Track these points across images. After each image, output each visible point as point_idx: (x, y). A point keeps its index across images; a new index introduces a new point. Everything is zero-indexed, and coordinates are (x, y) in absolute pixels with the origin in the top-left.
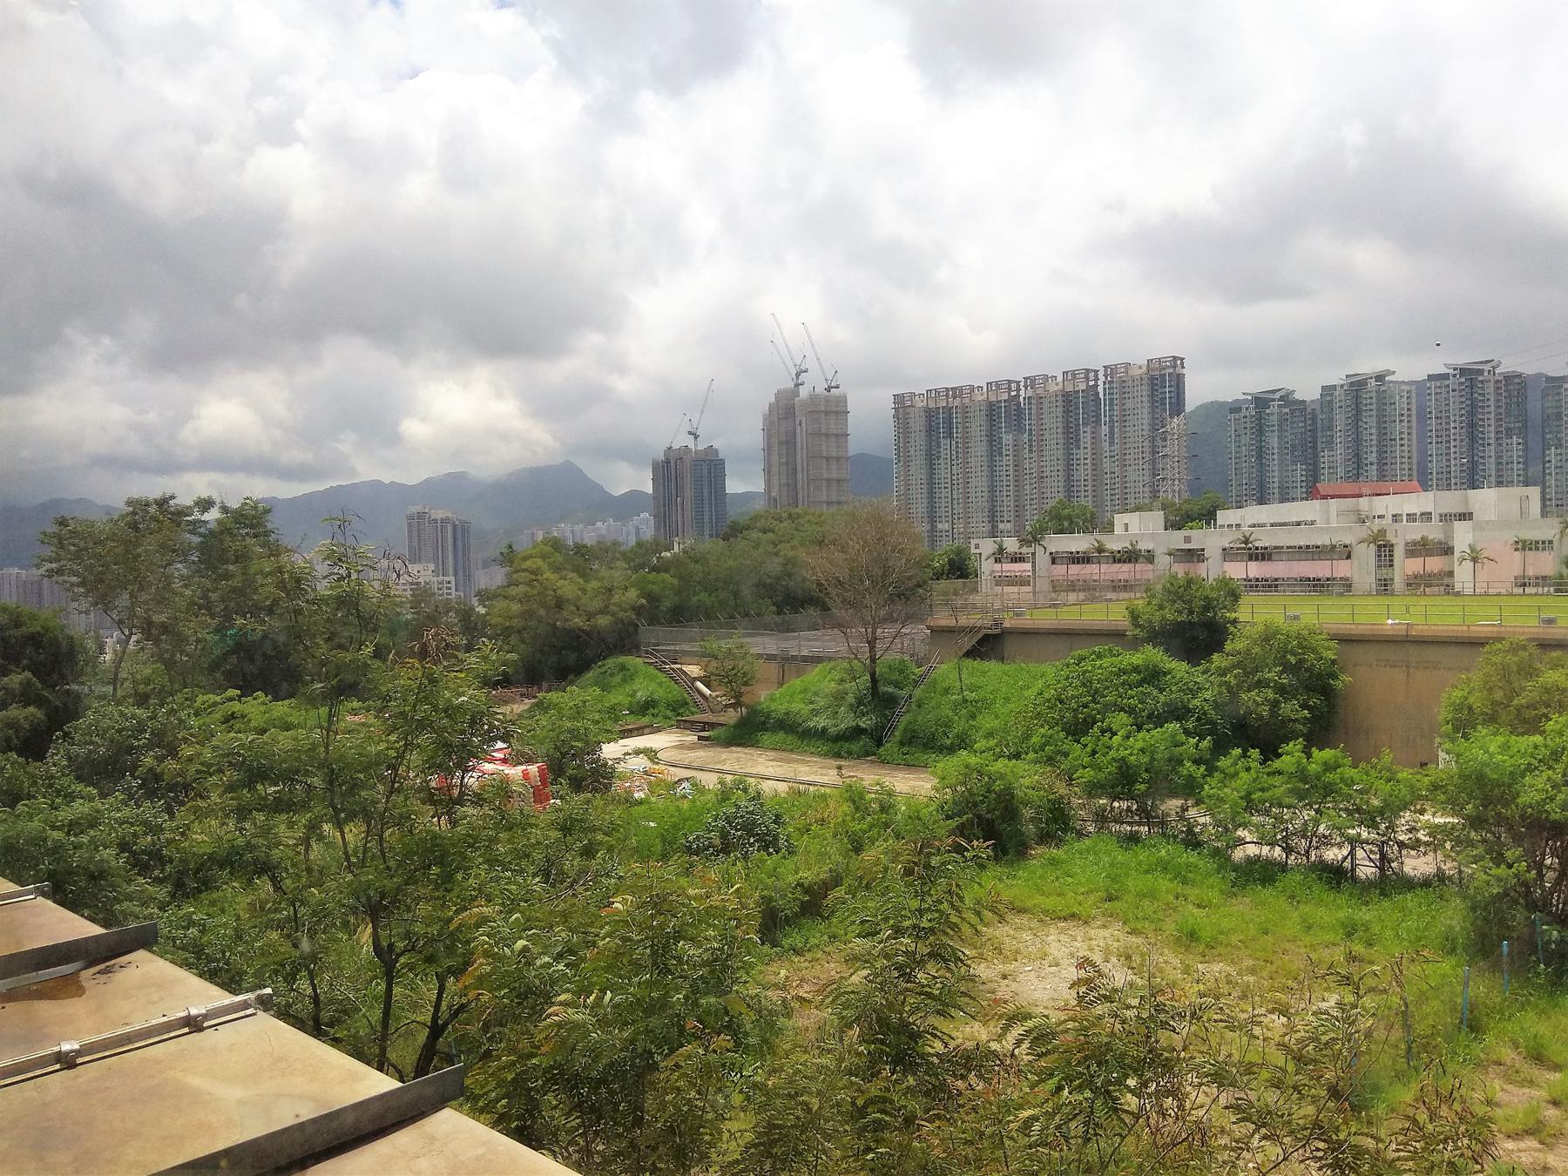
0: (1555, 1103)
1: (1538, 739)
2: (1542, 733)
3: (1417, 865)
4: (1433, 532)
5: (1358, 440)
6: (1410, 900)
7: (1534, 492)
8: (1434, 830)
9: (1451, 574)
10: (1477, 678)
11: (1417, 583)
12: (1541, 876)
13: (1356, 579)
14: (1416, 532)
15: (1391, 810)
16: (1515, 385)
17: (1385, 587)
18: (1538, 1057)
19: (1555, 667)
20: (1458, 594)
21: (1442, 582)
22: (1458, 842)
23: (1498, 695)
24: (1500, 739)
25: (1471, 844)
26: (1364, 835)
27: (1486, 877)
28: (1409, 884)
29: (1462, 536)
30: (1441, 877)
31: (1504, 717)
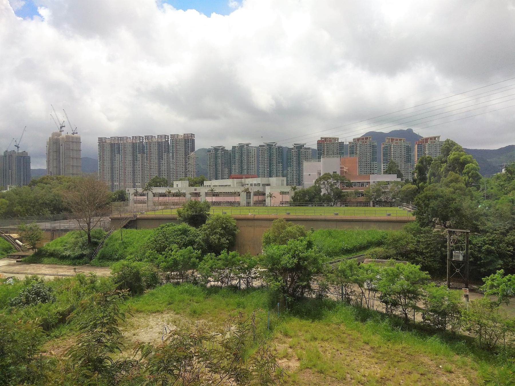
0: (291, 347)
1: (285, 246)
2: (287, 244)
3: (256, 283)
4: (260, 189)
5: (242, 162)
6: (254, 294)
7: (285, 179)
8: (261, 273)
9: (265, 201)
10: (271, 229)
11: (256, 203)
12: (287, 284)
13: (241, 202)
14: (256, 189)
15: (250, 268)
16: (280, 149)
17: (248, 204)
18: (286, 335)
19: (290, 226)
20: (266, 206)
21: (262, 203)
22: (267, 276)
23: (276, 234)
24: (277, 246)
25: (270, 276)
26: (243, 276)
27: (274, 285)
28: (254, 289)
29: (268, 190)
30: (262, 286)
31: (278, 240)
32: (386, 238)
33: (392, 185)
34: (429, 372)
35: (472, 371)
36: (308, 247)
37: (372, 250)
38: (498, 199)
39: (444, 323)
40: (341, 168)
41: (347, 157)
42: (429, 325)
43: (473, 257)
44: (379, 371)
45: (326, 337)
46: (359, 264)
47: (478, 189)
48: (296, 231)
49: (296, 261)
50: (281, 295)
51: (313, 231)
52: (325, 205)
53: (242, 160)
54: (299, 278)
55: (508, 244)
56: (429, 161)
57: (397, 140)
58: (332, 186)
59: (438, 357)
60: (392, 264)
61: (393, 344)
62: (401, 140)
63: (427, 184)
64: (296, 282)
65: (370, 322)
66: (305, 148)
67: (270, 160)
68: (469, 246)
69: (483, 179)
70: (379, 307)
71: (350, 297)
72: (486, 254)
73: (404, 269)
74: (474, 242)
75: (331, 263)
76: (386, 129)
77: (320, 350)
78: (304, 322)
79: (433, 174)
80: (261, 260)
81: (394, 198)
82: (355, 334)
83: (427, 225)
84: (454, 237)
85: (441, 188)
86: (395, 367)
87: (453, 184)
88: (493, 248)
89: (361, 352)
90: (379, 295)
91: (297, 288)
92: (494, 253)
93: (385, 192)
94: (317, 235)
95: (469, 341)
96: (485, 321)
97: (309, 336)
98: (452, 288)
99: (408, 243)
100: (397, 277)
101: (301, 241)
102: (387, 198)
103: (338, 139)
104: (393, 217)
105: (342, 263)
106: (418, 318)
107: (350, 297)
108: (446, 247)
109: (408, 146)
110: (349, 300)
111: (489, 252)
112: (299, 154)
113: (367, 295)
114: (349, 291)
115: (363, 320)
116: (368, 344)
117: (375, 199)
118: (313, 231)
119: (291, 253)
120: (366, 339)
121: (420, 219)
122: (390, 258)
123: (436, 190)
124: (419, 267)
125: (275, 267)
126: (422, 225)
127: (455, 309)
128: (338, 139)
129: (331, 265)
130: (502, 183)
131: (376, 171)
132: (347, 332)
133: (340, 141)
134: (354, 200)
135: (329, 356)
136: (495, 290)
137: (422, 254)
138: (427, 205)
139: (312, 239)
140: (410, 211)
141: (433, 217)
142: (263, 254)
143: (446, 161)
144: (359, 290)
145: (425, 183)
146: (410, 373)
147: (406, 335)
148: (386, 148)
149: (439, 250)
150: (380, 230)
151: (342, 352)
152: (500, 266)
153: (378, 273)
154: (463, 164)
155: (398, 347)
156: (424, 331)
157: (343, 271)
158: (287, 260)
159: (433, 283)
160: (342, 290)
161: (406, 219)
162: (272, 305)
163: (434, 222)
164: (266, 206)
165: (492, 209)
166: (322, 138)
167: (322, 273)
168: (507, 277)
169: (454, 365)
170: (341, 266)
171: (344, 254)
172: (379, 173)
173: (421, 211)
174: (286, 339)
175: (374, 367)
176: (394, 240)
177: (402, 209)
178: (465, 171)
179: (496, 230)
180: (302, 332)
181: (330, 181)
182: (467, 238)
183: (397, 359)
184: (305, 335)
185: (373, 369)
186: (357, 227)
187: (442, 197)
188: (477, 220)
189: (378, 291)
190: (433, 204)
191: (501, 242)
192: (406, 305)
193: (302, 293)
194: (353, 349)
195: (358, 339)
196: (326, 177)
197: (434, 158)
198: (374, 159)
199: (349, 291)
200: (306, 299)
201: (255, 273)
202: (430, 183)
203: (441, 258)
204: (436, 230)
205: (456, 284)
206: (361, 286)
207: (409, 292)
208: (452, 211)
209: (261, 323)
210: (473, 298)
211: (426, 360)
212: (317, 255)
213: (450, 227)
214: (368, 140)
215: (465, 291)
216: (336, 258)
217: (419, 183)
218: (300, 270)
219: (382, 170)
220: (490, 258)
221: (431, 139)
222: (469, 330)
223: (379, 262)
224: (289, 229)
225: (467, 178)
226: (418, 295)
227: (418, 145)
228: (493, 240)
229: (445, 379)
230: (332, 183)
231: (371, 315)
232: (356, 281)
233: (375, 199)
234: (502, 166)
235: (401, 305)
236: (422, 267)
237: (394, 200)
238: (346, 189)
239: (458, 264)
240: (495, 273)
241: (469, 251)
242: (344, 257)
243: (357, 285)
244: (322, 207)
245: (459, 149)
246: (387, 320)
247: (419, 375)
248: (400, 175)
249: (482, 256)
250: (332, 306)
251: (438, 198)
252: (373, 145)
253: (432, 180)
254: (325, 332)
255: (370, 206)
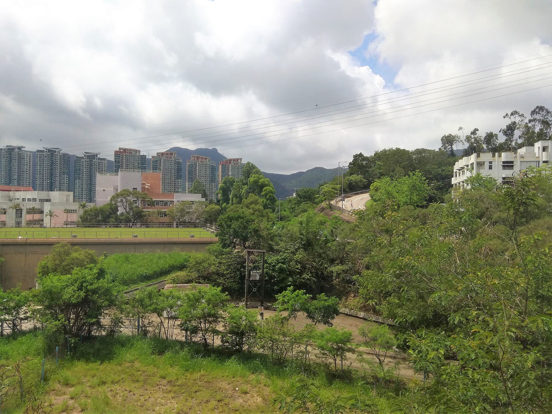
0: (72, 398)
1: (69, 276)
2: (71, 274)
3: (26, 326)
4: (37, 205)
5: (10, 170)
6: (23, 339)
7: (71, 194)
8: (34, 311)
9: (42, 220)
10: (50, 256)
11: (30, 223)
12: (69, 322)
13: (7, 222)
14: (31, 205)
15: (18, 306)
16: (66, 158)
17: (18, 224)
18: (67, 384)
19: (76, 251)
20: (45, 227)
21: (40, 223)
22: (42, 315)
23: (57, 262)
24: (57, 277)
25: (46, 315)
26: (7, 317)
27: (52, 325)
28: (24, 333)
29: (47, 207)
30: (35, 328)
31: (59, 270)
32: (188, 261)
33: (196, 205)
34: (226, 397)
35: (265, 388)
36: (99, 276)
37: (173, 275)
38: (290, 221)
39: (240, 344)
40: (143, 184)
41: (149, 172)
42: (227, 348)
43: (268, 276)
44: (176, 406)
45: (117, 378)
46: (159, 290)
47: (274, 211)
48: (83, 257)
49: (82, 294)
50: (62, 336)
51: (106, 256)
52: (122, 226)
53: (10, 167)
54: (86, 314)
55: (297, 262)
56: (232, 183)
57: (202, 158)
58: (131, 204)
59: (234, 379)
60: (195, 288)
61: (192, 373)
62: (206, 159)
63: (230, 205)
64: (81, 319)
65: (168, 354)
66: (100, 159)
67: (51, 169)
68: (265, 265)
69: (278, 202)
70: (177, 334)
71: (148, 328)
72: (279, 273)
73: (205, 293)
74: (269, 261)
75: (126, 293)
76: (191, 146)
77: (109, 394)
78: (91, 365)
79: (235, 196)
80: (34, 296)
81: (199, 219)
82: (151, 369)
83: (229, 246)
84: (252, 257)
85: (248, 208)
86: (192, 398)
87: (253, 205)
88: (285, 266)
89: (157, 388)
90: (179, 323)
91: (83, 326)
92: (285, 271)
93: (189, 212)
94: (109, 261)
95: (263, 358)
96: (277, 337)
97: (96, 380)
98: (249, 308)
99: (210, 265)
100: (199, 302)
101: (91, 269)
102: (191, 219)
103: (139, 151)
104: (197, 238)
105: (140, 291)
106: (217, 342)
107: (148, 328)
108: (244, 267)
109: (212, 166)
110: (145, 333)
111: (281, 270)
112: (91, 165)
113: (166, 325)
114: (146, 322)
115: (161, 353)
116: (165, 378)
117: (179, 220)
118: (106, 256)
119: (76, 285)
120: (162, 373)
121: (222, 241)
122: (192, 282)
123: (238, 211)
124: (220, 289)
125: (52, 302)
126: (224, 247)
127: (252, 329)
128: (139, 151)
129: (128, 295)
130: (293, 206)
131: (180, 190)
132: (141, 369)
133: (141, 154)
134: (156, 221)
135: (120, 399)
136: (285, 306)
137: (223, 275)
138: (229, 226)
139: (105, 266)
140: (213, 232)
141: (234, 238)
142: (38, 287)
143: (247, 184)
144: (158, 320)
145: (228, 203)
146: (208, 401)
147: (205, 362)
148: (191, 166)
149: (239, 270)
150: (183, 253)
151: (135, 392)
152: (290, 283)
153: (179, 298)
154: (262, 186)
155: (197, 375)
156: (223, 354)
157: (141, 301)
158: (70, 294)
159: (233, 304)
160: (139, 322)
161: (207, 240)
162: (49, 351)
163: (235, 243)
164: (45, 227)
165: (284, 230)
166: (120, 149)
167: (115, 305)
168: (296, 293)
169: (249, 385)
170: (138, 295)
171: (142, 282)
172: (184, 191)
173: (223, 232)
174: (65, 389)
175: (171, 402)
176: (197, 263)
177: (205, 230)
178: (263, 193)
179: (287, 250)
180: (88, 378)
181: (129, 198)
182: (264, 258)
183: (194, 389)
184: (91, 380)
185: (170, 404)
186: (159, 251)
187: (243, 218)
188: (272, 240)
189: (178, 318)
190: (235, 225)
191: (291, 261)
192: (206, 330)
193: (90, 331)
194: (148, 387)
195: (154, 375)
196: (125, 194)
197: (236, 180)
198: (179, 177)
199: (146, 322)
200: (95, 337)
201: (26, 313)
202: (232, 204)
203: (240, 279)
204: (236, 250)
205: (253, 303)
206: (160, 315)
207: (210, 315)
208: (251, 232)
209: (31, 375)
210: (268, 315)
211: (224, 385)
212: (111, 285)
213: (249, 247)
214: (173, 156)
215: (260, 309)
216: (133, 287)
217: (222, 204)
218: (89, 304)
219: (187, 189)
220: (282, 276)
221: (234, 160)
222: (263, 347)
223: (181, 287)
224: (75, 255)
225: (265, 200)
226: (218, 318)
227: (222, 165)
228: (285, 259)
229: (241, 401)
230: (132, 201)
231: (170, 346)
232: (155, 311)
233: (179, 220)
234: (293, 191)
235: (202, 330)
236: (222, 289)
237: (198, 221)
238: (148, 208)
239: (255, 282)
240: (286, 290)
241: (265, 270)
242: (143, 284)
243: (156, 315)
244: (118, 229)
245: (258, 172)
246: (186, 349)
247: (217, 402)
248: (204, 195)
249: (275, 274)
250: (125, 343)
251: (240, 219)
252: (178, 162)
253: (234, 201)
254: (116, 373)
255: (173, 227)
